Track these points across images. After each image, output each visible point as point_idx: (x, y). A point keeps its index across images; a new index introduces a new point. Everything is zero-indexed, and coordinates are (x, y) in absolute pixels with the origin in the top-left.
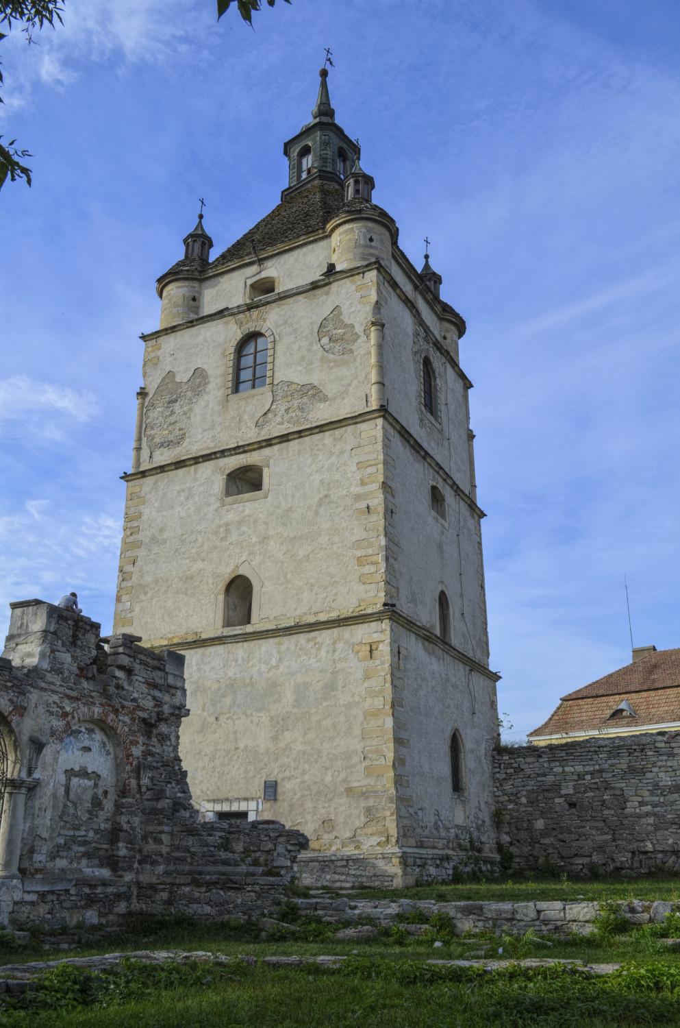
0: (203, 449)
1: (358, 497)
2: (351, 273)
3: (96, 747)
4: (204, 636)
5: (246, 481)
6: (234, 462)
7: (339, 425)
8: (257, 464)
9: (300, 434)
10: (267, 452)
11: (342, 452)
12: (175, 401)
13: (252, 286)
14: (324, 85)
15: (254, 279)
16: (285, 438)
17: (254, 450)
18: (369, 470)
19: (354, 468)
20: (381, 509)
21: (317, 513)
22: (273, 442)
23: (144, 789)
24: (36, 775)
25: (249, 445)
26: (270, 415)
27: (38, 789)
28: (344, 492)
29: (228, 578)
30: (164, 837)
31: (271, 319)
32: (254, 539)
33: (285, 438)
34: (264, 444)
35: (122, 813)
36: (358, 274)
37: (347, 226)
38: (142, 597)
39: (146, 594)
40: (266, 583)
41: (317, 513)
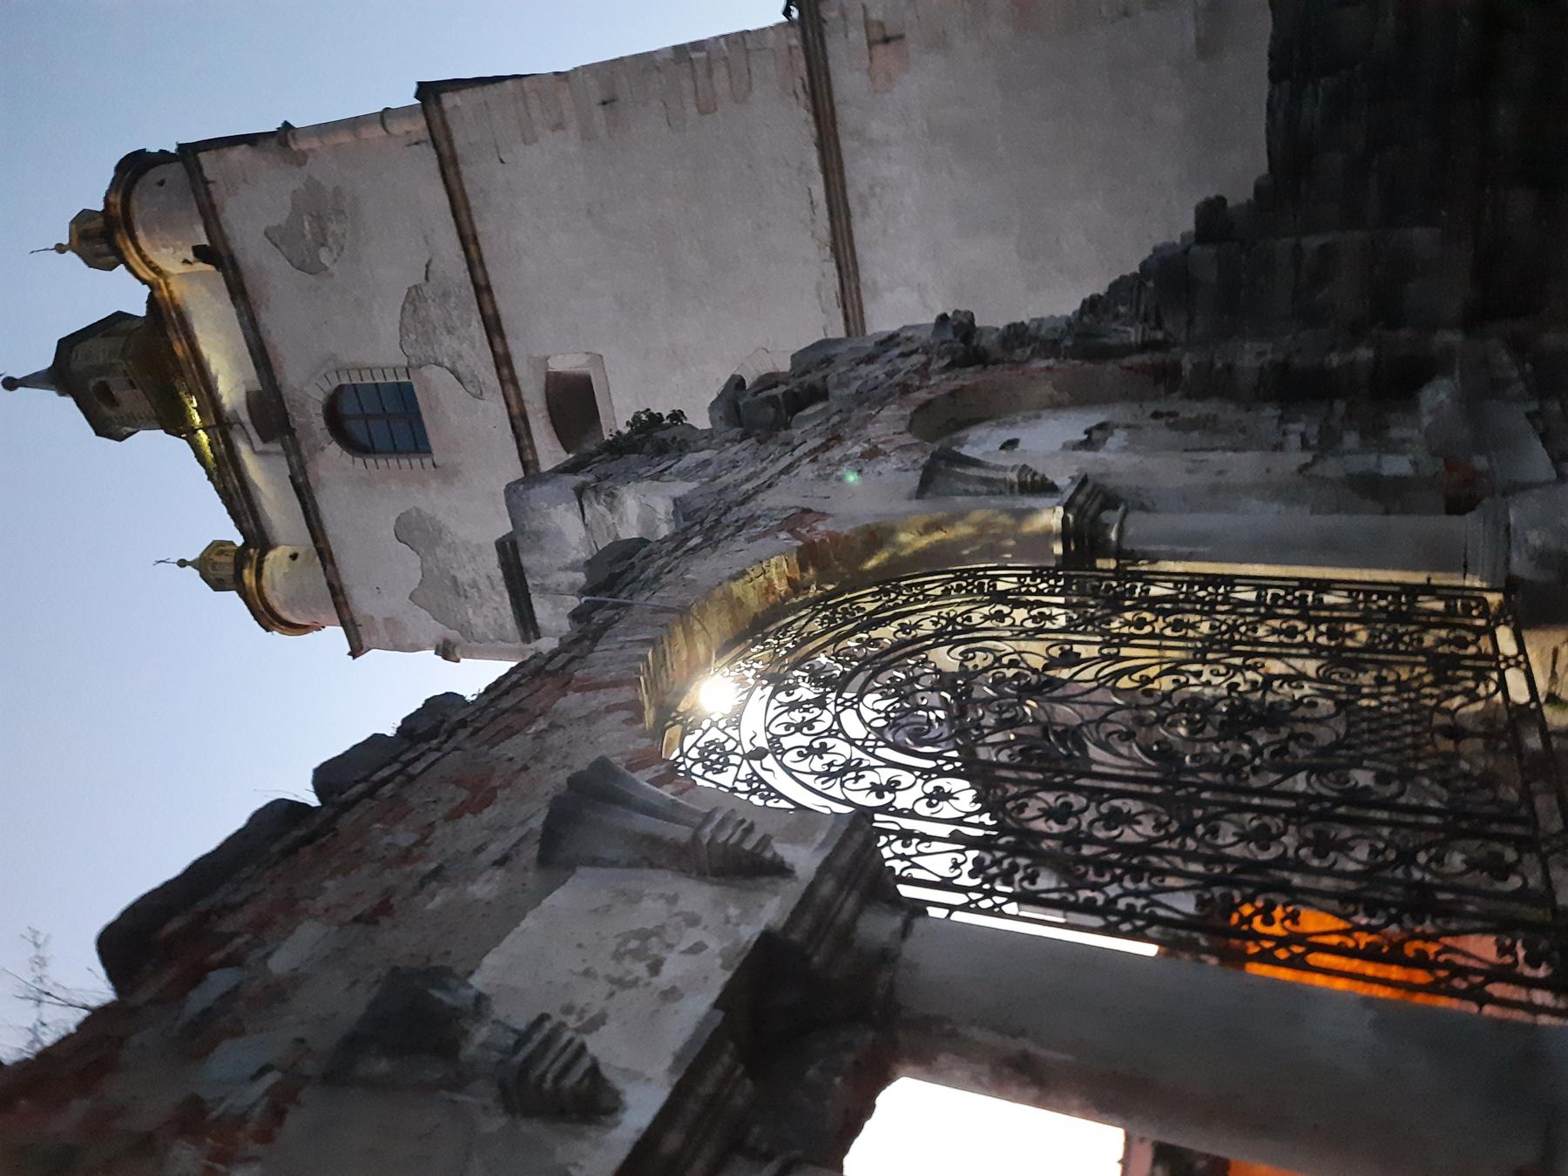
1: (587, 136)
2: (210, 215)
3: (1006, 434)
7: (458, 196)
8: (542, 385)
9: (482, 290)
10: (521, 369)
12: (454, 579)
13: (265, 440)
14: (28, 382)
15: (255, 437)
16: (493, 327)
17: (519, 394)
22: (500, 350)
23: (1159, 335)
24: (1062, 481)
25: (508, 404)
26: (461, 368)
27: (1110, 483)
30: (1312, 243)
31: (307, 391)
33: (493, 327)
34: (505, 371)
35: (1229, 368)
36: (208, 194)
37: (140, 233)
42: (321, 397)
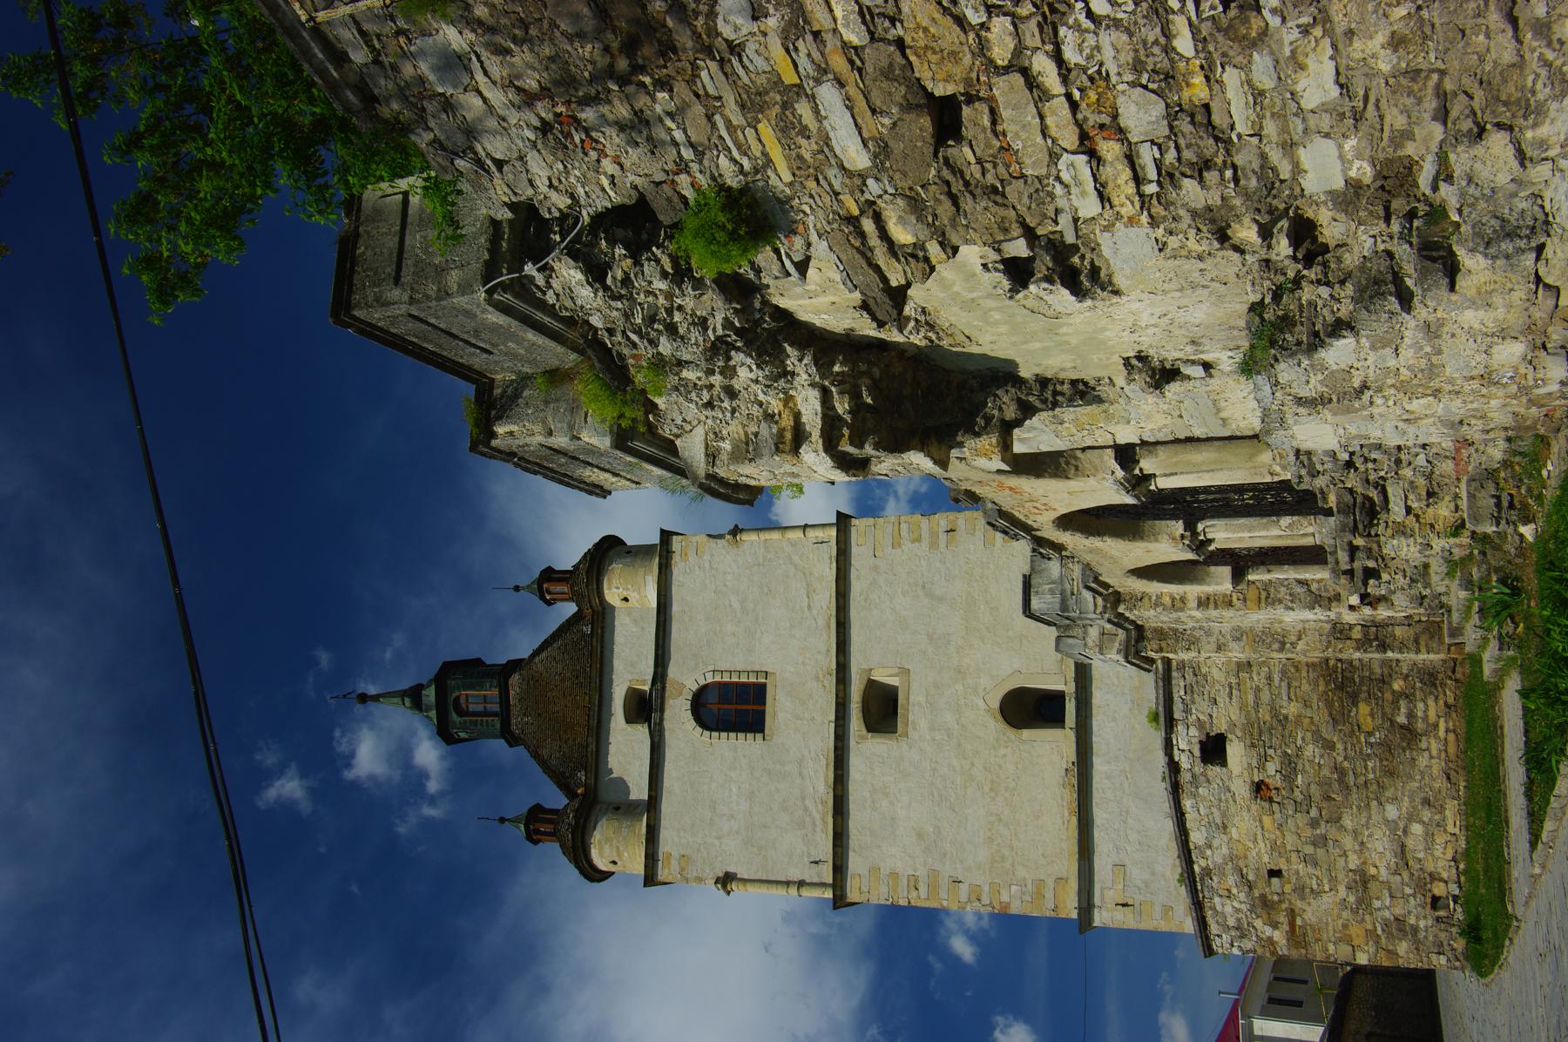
0: (826, 777)
1: (934, 545)
4: (1073, 758)
5: (883, 709)
6: (856, 723)
11: (875, 568)
18: (904, 532)
19: (898, 551)
20: (952, 516)
21: (941, 599)
28: (924, 563)
29: (1002, 726)
32: (960, 687)
38: (1007, 865)
39: (1003, 858)
40: (1016, 666)
41: (941, 599)
42: (695, 688)
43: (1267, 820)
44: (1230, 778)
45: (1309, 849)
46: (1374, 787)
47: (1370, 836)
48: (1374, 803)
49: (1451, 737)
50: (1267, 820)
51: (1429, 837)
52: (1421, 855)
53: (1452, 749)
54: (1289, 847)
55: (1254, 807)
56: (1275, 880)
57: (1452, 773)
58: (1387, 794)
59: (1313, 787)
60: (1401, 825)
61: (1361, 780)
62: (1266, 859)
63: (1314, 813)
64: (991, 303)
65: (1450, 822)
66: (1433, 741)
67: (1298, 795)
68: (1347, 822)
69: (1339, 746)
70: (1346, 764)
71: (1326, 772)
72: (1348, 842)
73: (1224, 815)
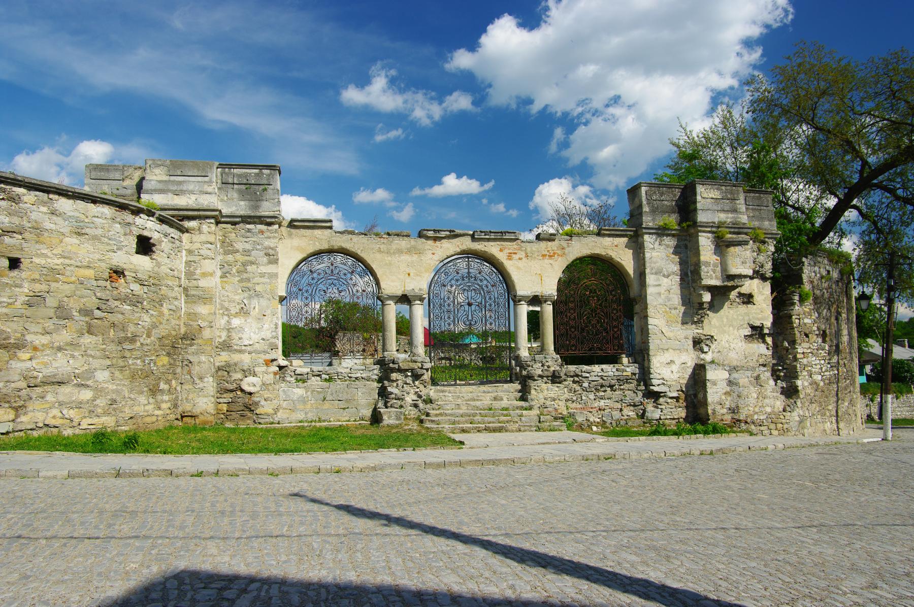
43: (90, 273)
44: (127, 253)
45: (51, 302)
46: (122, 364)
47: (73, 357)
48: (108, 362)
49: (154, 419)
50: (90, 273)
51: (79, 405)
52: (49, 397)
53: (148, 420)
54: (53, 285)
55: (103, 265)
56: (6, 263)
57: (134, 421)
58: (117, 374)
59: (120, 316)
60: (89, 383)
61: (127, 354)
62: (36, 260)
63: (98, 313)
64: (746, 318)
65: (95, 420)
66: (152, 406)
67: (113, 304)
68: (87, 339)
69: (148, 341)
70: (138, 344)
71: (131, 328)
72: (65, 336)
73: (95, 238)
